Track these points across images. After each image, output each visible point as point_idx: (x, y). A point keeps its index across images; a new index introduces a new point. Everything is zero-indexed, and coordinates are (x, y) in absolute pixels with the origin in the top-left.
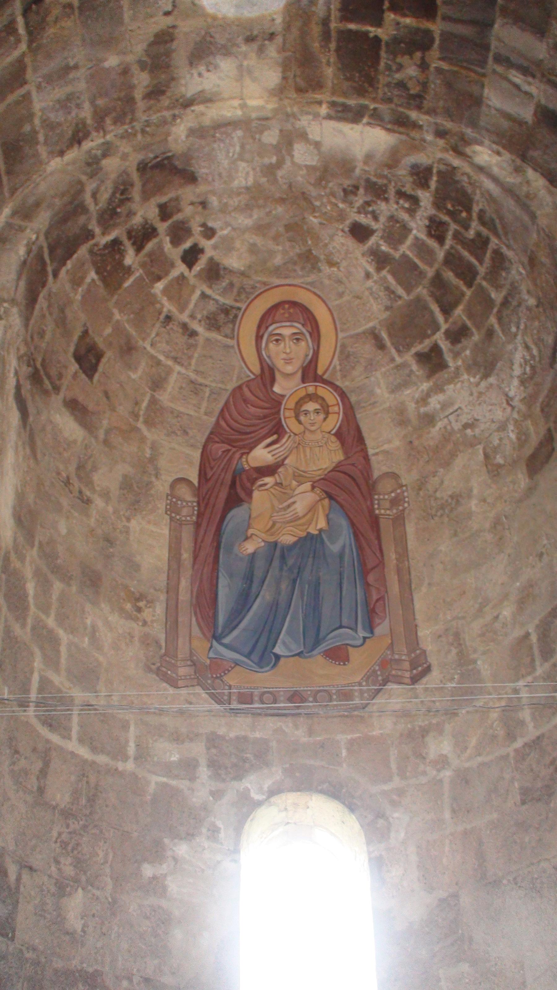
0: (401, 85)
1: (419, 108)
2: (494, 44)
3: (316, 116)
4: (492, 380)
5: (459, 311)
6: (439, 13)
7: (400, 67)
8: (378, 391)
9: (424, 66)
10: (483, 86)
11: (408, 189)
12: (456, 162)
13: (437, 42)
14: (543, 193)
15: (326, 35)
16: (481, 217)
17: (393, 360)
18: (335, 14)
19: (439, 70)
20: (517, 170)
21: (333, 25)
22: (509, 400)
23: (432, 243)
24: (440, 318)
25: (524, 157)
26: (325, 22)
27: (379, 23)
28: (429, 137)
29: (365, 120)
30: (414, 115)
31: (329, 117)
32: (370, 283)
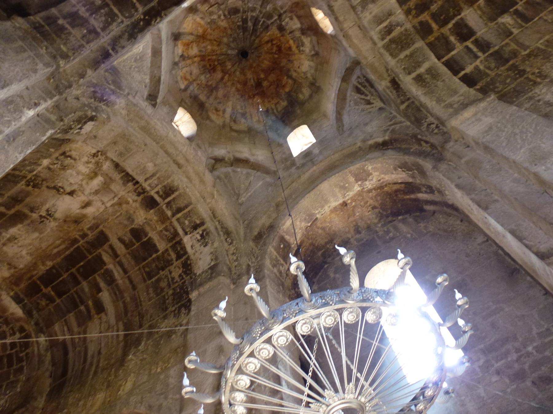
0: (38, 304)
1: (38, 312)
2: (67, 317)
6: (62, 299)
7: (41, 300)
9: (47, 305)
10: (57, 322)
11: (16, 329)
13: (56, 303)
14: (47, 362)
15: (30, 278)
16: (27, 354)
18: (37, 276)
19: (50, 309)
20: (47, 350)
21: (34, 278)
25: (51, 347)
26: (32, 276)
27: (46, 287)
28: (33, 323)
29: (21, 305)
30: (35, 312)
31: (12, 297)
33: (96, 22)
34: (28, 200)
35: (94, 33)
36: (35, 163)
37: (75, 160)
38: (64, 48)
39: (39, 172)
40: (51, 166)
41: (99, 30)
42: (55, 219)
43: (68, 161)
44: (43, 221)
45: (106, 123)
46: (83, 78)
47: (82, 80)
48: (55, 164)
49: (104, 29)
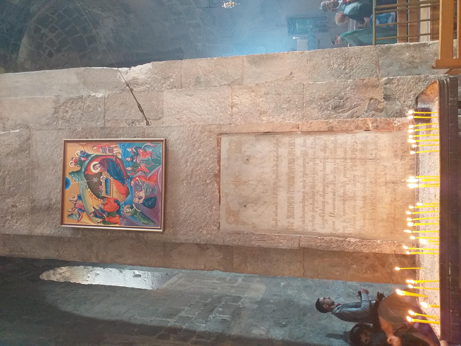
3: (16, 58)
4: (100, 22)
5: (78, 28)
8: (98, 58)
12: (36, 17)
17: (89, 52)
22: (108, 17)
23: (57, 32)
24: (79, 35)
29: (18, 43)
31: (18, 55)
32: (66, 55)
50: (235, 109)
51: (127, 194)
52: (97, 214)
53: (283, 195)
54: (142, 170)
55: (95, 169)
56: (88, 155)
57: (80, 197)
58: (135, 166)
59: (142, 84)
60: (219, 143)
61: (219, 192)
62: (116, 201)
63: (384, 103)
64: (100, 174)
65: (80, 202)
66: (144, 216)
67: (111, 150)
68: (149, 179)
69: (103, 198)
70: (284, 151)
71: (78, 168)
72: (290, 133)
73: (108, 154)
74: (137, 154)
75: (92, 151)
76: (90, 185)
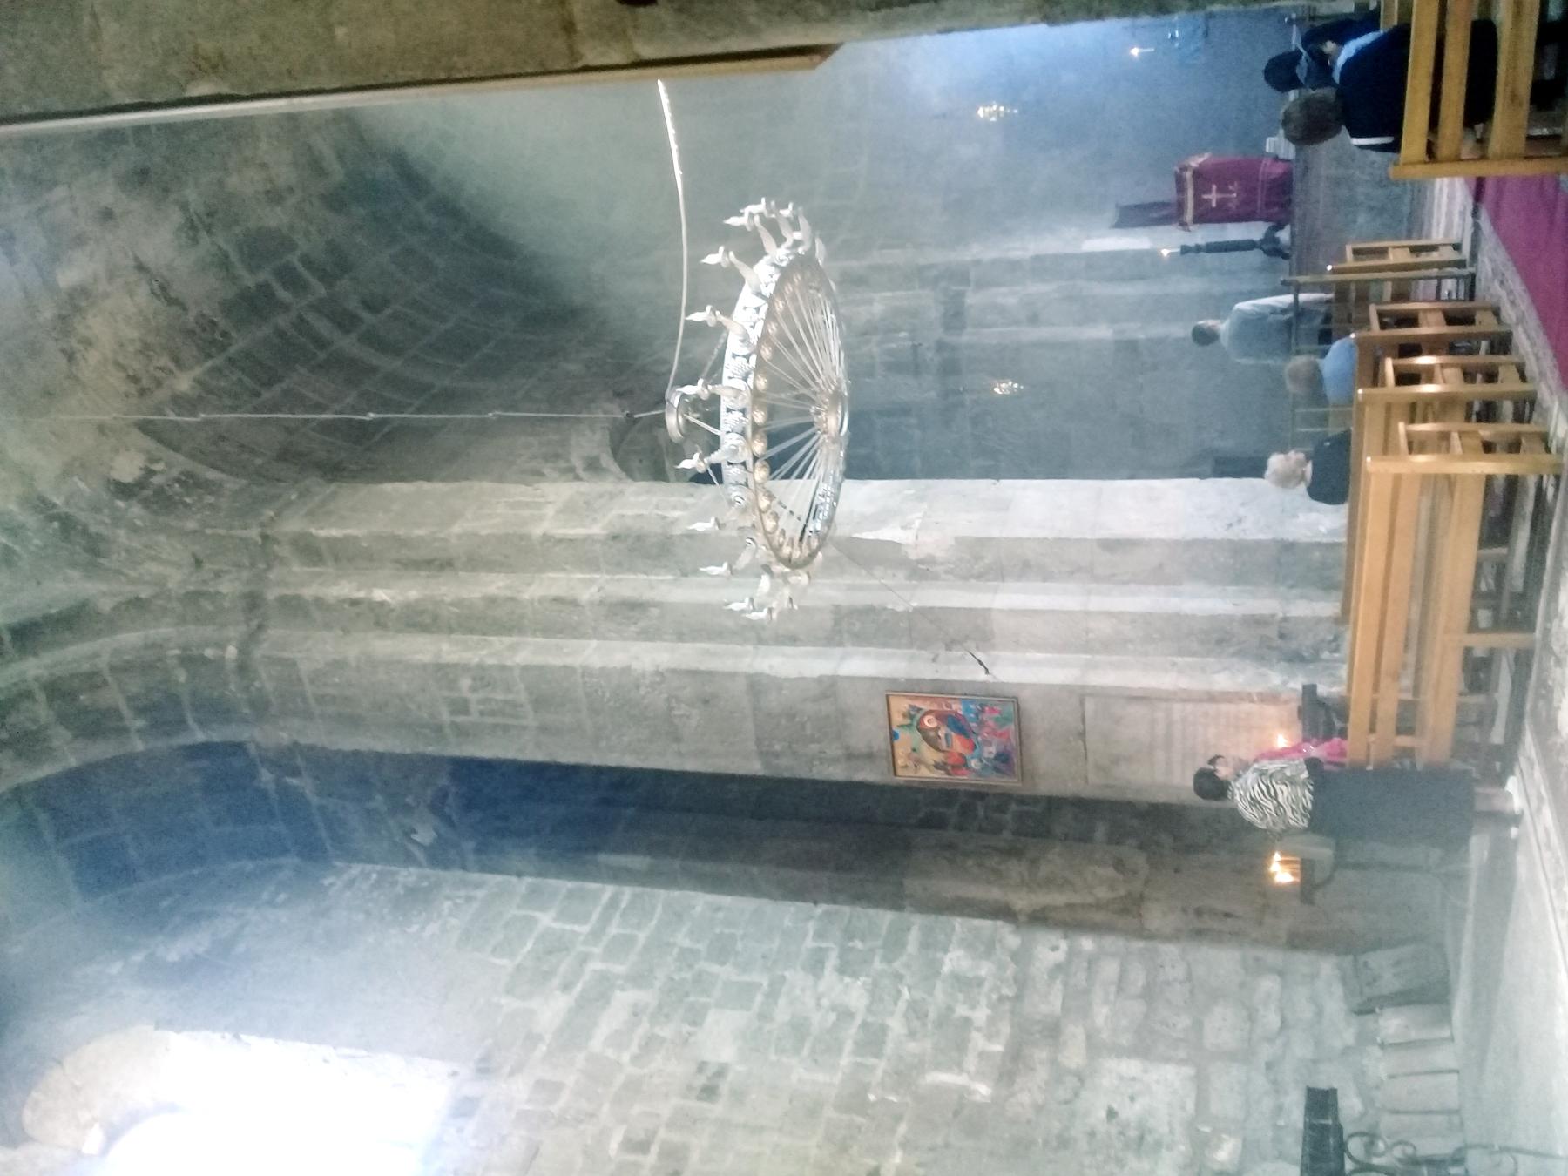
33: (42, 711)
34: (231, 293)
35: (57, 690)
36: (210, 392)
37: (118, 365)
38: (182, 676)
39: (198, 362)
40: (172, 366)
41: (41, 697)
42: (184, 207)
43: (136, 365)
44: (210, 215)
45: (77, 464)
46: (138, 599)
47: (143, 596)
48: (160, 368)
49: (28, 695)
50: (1091, 635)
51: (974, 747)
52: (937, 766)
53: (1160, 755)
54: (989, 727)
55: (930, 723)
56: (919, 710)
57: (914, 750)
58: (981, 724)
59: (942, 564)
60: (1082, 703)
61: (1085, 749)
62: (961, 755)
63: (1279, 642)
64: (937, 729)
65: (915, 755)
66: (996, 769)
67: (949, 706)
68: (1001, 735)
69: (943, 751)
70: (1160, 715)
71: (908, 721)
72: (1167, 700)
73: (945, 709)
74: (983, 711)
75: (925, 706)
76: (927, 739)
